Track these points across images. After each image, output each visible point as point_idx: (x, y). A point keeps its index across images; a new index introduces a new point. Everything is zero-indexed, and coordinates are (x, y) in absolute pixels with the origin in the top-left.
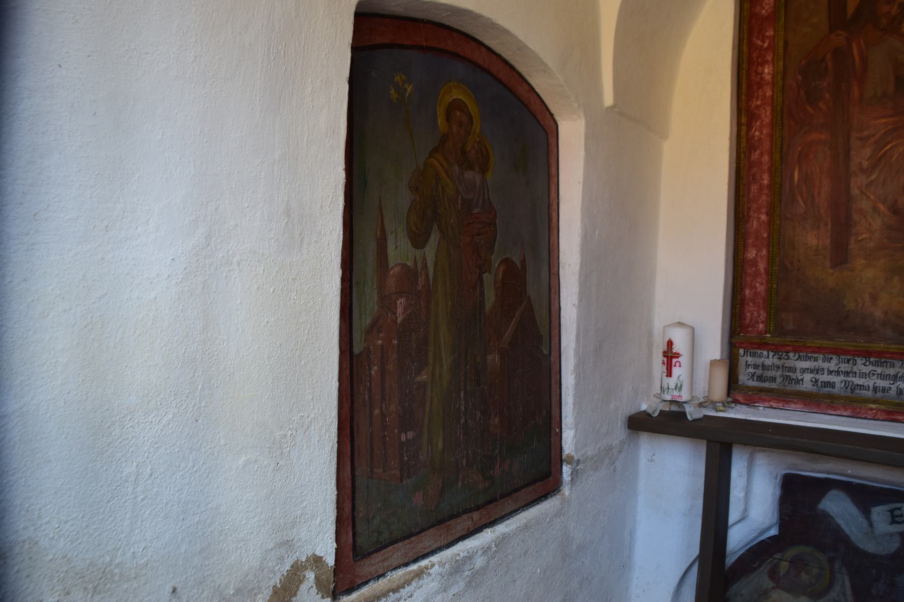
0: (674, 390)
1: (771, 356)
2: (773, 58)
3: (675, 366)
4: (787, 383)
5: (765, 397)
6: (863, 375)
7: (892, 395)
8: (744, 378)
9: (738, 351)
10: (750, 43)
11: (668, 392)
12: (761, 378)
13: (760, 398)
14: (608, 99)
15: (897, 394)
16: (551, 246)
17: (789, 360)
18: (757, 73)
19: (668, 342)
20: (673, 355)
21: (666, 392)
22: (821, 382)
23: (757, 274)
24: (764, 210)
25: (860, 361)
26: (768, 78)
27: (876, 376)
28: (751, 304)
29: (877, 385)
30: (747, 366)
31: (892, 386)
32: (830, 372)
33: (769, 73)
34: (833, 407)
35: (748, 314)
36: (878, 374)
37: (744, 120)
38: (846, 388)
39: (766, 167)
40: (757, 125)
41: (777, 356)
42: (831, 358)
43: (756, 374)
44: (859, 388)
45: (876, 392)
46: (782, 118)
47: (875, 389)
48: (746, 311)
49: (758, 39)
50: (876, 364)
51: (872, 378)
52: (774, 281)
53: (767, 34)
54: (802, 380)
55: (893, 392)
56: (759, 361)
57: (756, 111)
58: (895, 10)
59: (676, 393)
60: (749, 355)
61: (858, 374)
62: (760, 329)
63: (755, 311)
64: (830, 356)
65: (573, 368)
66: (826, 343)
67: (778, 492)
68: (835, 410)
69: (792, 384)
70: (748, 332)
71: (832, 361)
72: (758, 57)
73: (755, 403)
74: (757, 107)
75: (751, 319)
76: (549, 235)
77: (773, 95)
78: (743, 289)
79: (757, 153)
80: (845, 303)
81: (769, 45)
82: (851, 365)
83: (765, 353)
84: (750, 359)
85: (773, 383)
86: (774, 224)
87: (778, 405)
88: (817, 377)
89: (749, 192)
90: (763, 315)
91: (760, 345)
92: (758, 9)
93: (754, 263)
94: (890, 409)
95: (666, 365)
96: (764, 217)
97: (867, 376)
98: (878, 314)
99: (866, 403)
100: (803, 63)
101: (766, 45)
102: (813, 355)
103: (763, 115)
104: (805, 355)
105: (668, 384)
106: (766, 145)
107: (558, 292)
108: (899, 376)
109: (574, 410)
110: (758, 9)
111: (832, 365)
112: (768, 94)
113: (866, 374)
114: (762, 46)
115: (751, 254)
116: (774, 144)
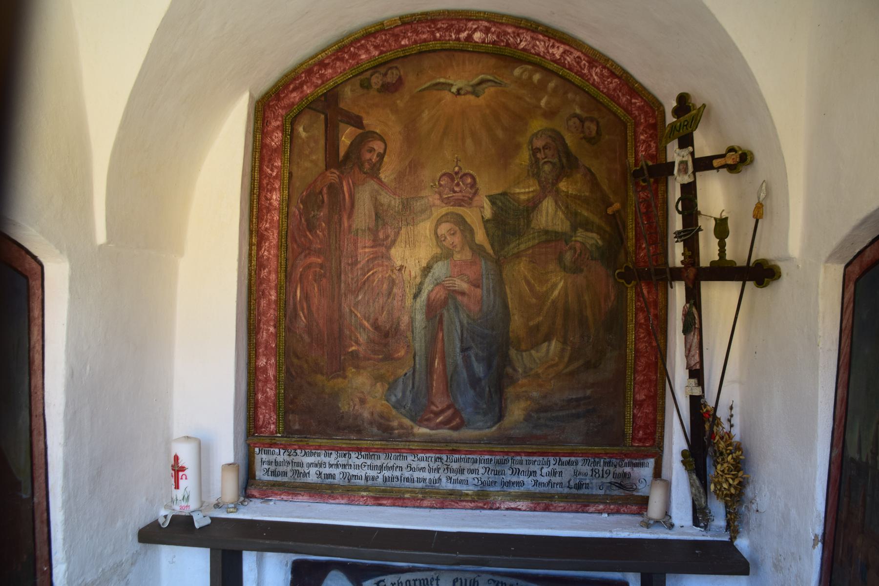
0: (182, 501)
1: (282, 454)
2: (280, 187)
3: (182, 479)
4: (296, 477)
5: (276, 492)
6: (358, 467)
7: (379, 482)
8: (260, 474)
9: (254, 450)
10: (261, 170)
11: (176, 502)
12: (274, 473)
13: (272, 492)
14: (101, 237)
15: (383, 481)
16: (32, 388)
17: (297, 456)
18: (267, 199)
19: (175, 456)
20: (180, 469)
21: (175, 503)
22: (324, 474)
23: (267, 381)
24: (272, 324)
25: (354, 455)
26: (275, 203)
27: (366, 467)
28: (263, 408)
29: (368, 474)
30: (263, 462)
31: (379, 475)
32: (331, 466)
33: (276, 200)
34: (333, 497)
35: (261, 416)
36: (368, 465)
37: (254, 240)
38: (344, 479)
39: (273, 284)
40: (266, 246)
41: (287, 453)
42: (331, 453)
43: (270, 470)
44: (354, 478)
45: (367, 481)
46: (286, 241)
47: (367, 478)
48: (259, 414)
49: (268, 168)
50: (366, 457)
51: (364, 469)
52: (281, 387)
53: (276, 164)
54: (309, 473)
55: (380, 480)
56: (272, 458)
57: (265, 233)
58: (375, 158)
59: (184, 504)
60: (263, 453)
61: (353, 466)
62: (271, 430)
63: (266, 413)
64: (330, 452)
65: (61, 505)
66: (324, 442)
67: (290, 577)
68: (334, 499)
69: (300, 477)
70: (261, 432)
71: (331, 456)
72: (267, 184)
73: (269, 497)
74: (266, 229)
75: (264, 421)
76: (30, 375)
77: (279, 220)
78: (255, 394)
79: (265, 271)
80: (340, 405)
81: (277, 174)
82: (347, 458)
83: (277, 450)
84: (264, 457)
85: (285, 477)
86: (280, 336)
87: (288, 497)
88: (321, 470)
89: (259, 305)
90: (274, 417)
91: (271, 445)
92: (268, 141)
93: (265, 370)
94: (378, 496)
95: (174, 477)
96: (272, 329)
97: (360, 468)
98: (366, 415)
99: (359, 491)
100: (304, 193)
101: (274, 174)
102: (317, 451)
103: (271, 238)
104: (310, 451)
105: (176, 495)
106: (273, 264)
107: (43, 432)
108: (384, 466)
109: (64, 545)
110: (268, 141)
111: (332, 459)
112: (275, 218)
113: (359, 466)
114: (271, 174)
115: (262, 362)
116: (279, 264)
